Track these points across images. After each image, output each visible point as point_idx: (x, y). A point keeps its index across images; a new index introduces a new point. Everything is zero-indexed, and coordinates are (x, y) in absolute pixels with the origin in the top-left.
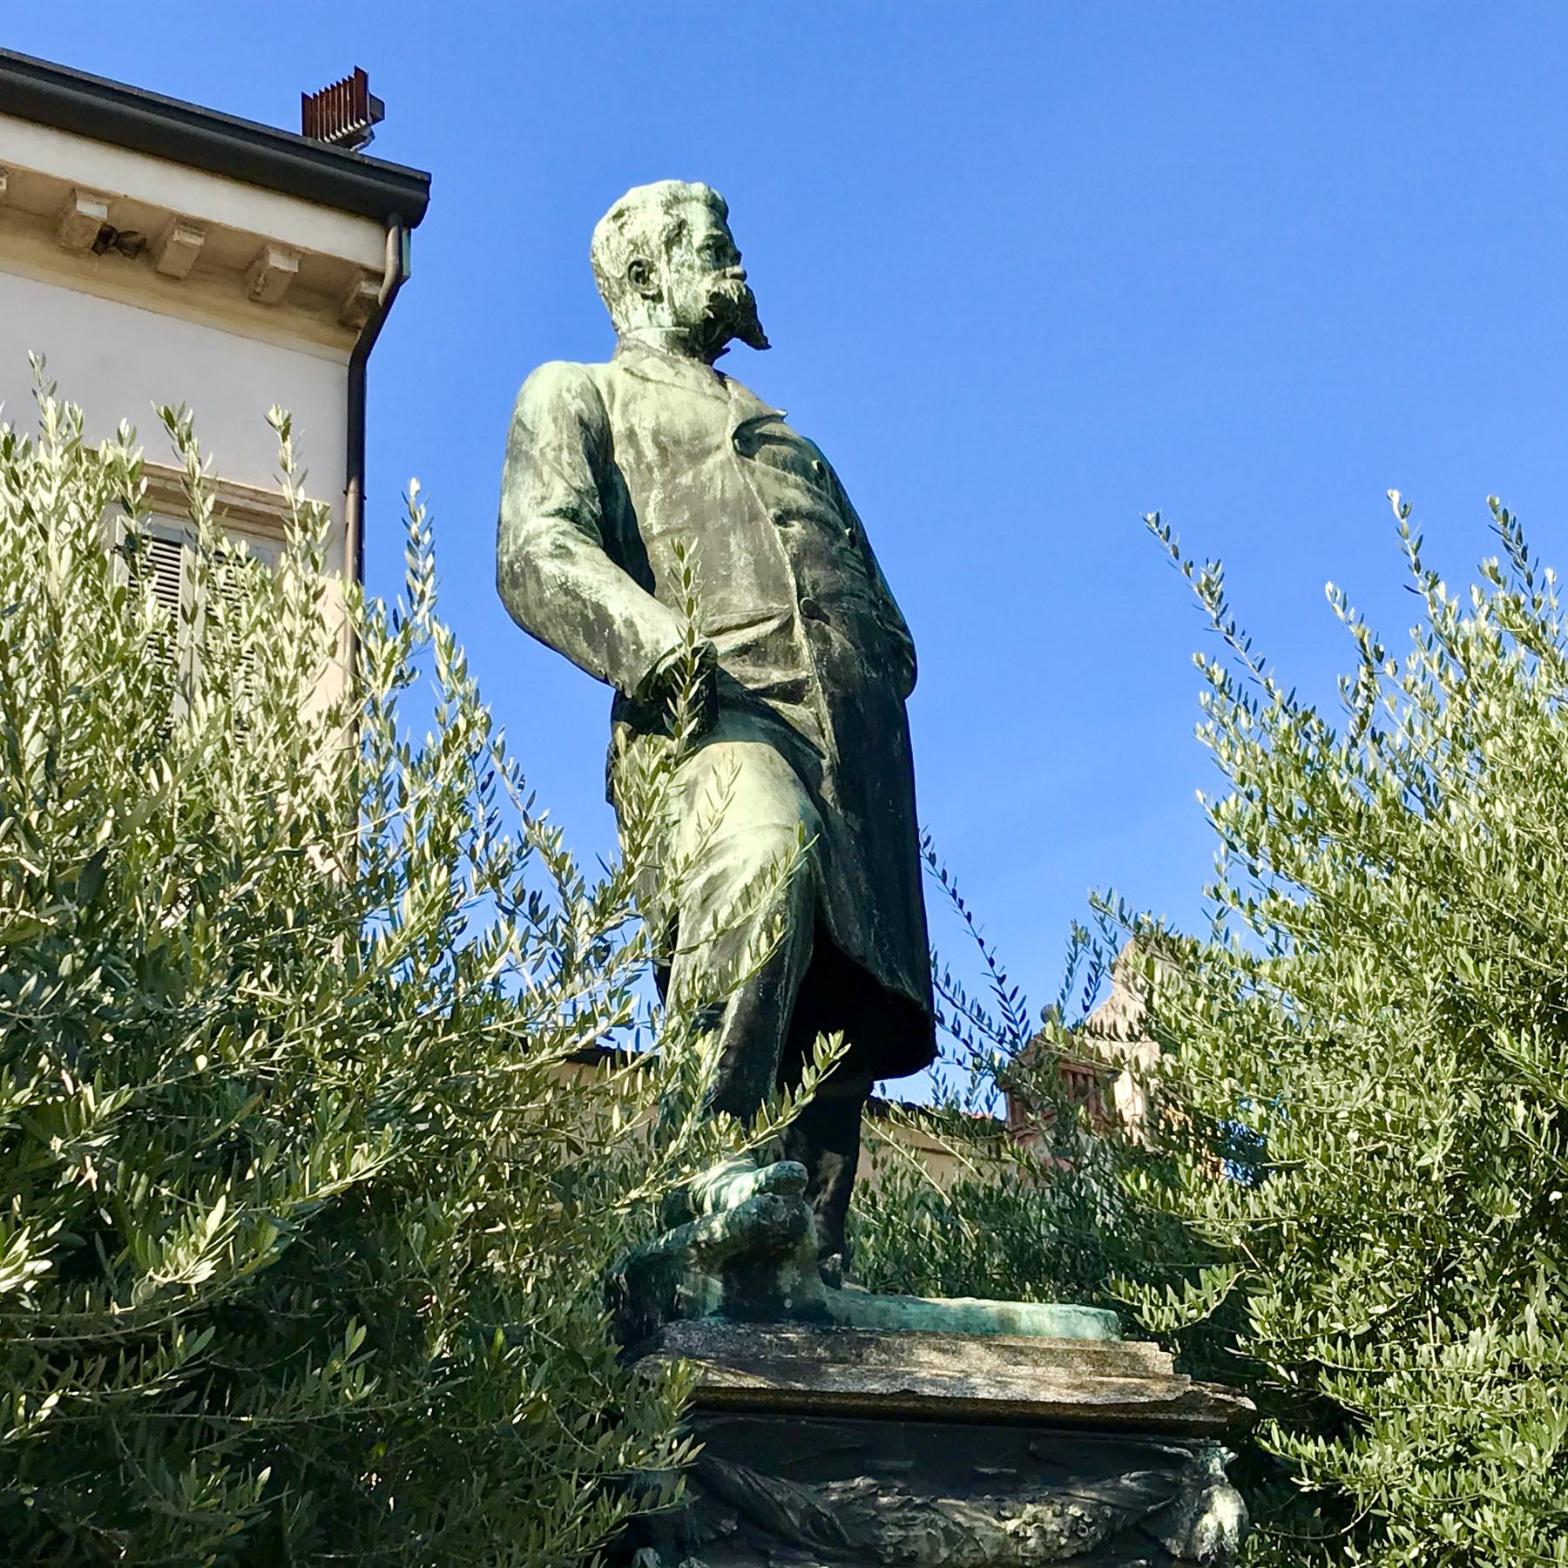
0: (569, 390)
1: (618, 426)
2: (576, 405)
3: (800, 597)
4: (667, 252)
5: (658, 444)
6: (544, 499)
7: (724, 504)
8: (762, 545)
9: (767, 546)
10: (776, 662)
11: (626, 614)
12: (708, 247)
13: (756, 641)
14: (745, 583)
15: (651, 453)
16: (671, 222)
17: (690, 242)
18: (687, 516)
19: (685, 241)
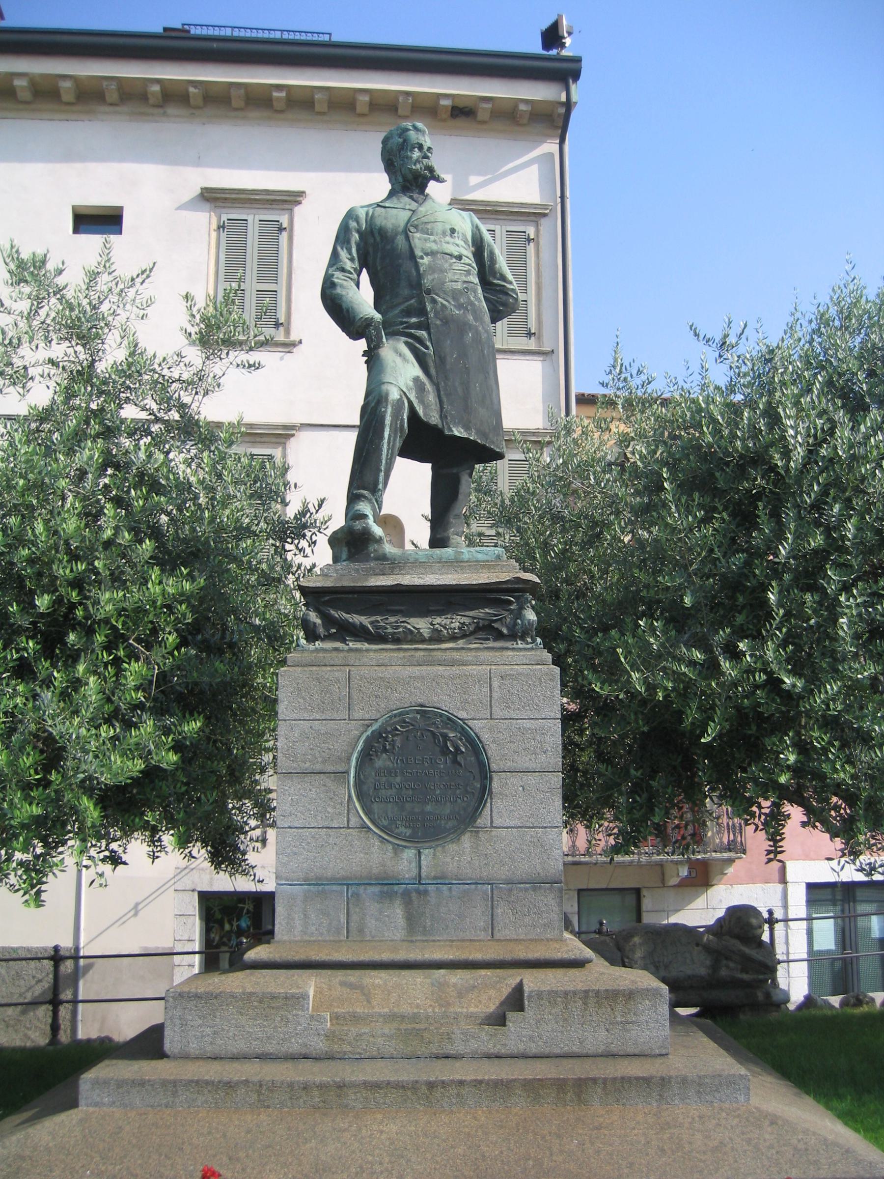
15: (378, 239)
16: (401, 140)
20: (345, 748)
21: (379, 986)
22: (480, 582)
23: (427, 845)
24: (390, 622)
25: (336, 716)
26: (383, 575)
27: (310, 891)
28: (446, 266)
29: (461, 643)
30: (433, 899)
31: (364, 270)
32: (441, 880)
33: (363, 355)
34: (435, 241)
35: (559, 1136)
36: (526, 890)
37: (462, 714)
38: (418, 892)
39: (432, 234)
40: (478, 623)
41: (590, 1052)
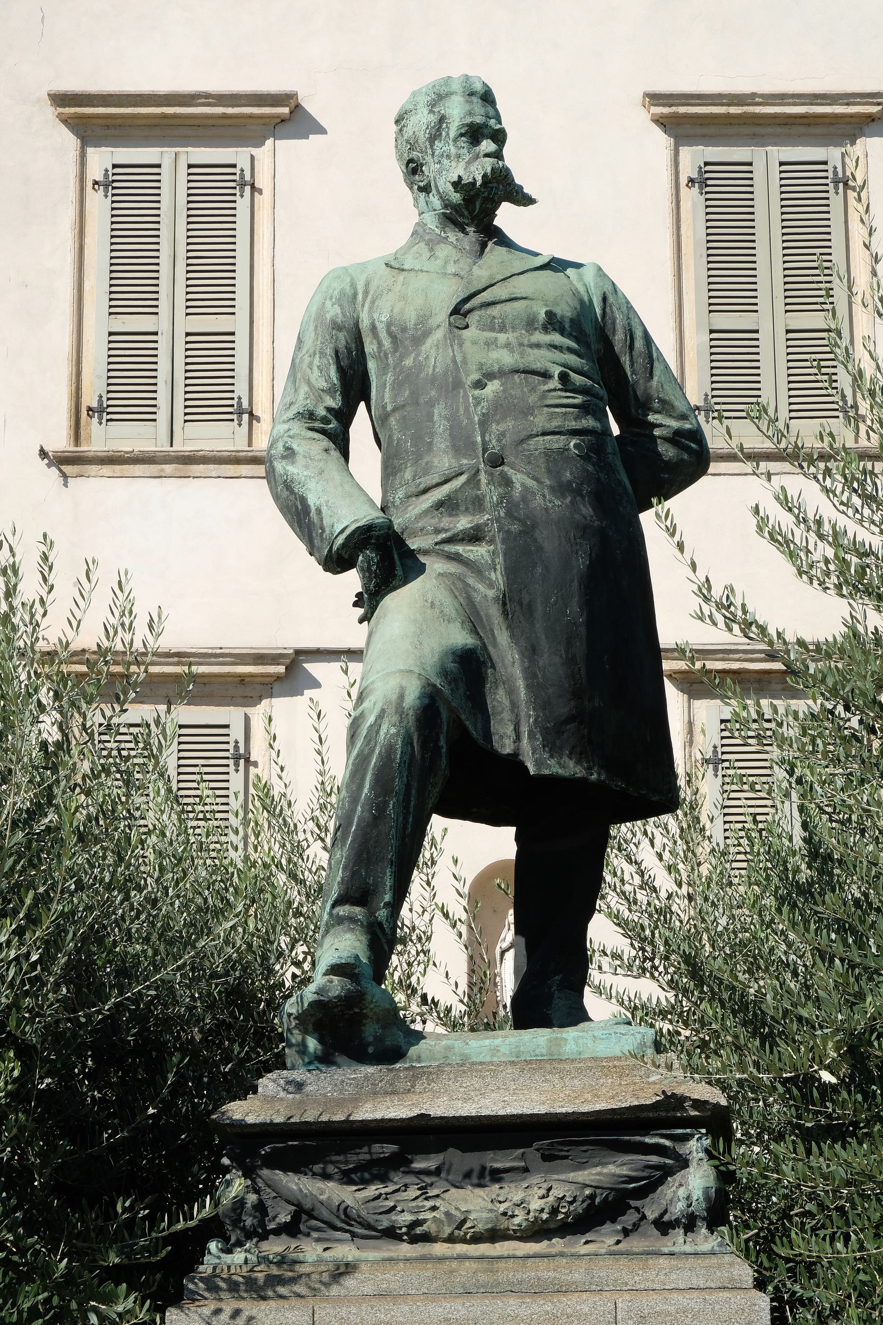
0: (331, 298)
1: (365, 324)
2: (333, 312)
3: (485, 450)
4: (432, 147)
5: (390, 334)
6: (291, 404)
7: (433, 379)
8: (458, 410)
9: (462, 411)
10: (467, 509)
11: (318, 503)
12: (462, 135)
13: (449, 496)
14: (443, 446)
15: (387, 343)
16: (433, 118)
17: (448, 134)
18: (407, 393)
19: (444, 133)
22: (598, 1107)
26: (394, 1093)
28: (532, 399)
29: (558, 1245)
31: (362, 405)
33: (356, 604)
34: (508, 345)
39: (502, 329)
40: (592, 1197)
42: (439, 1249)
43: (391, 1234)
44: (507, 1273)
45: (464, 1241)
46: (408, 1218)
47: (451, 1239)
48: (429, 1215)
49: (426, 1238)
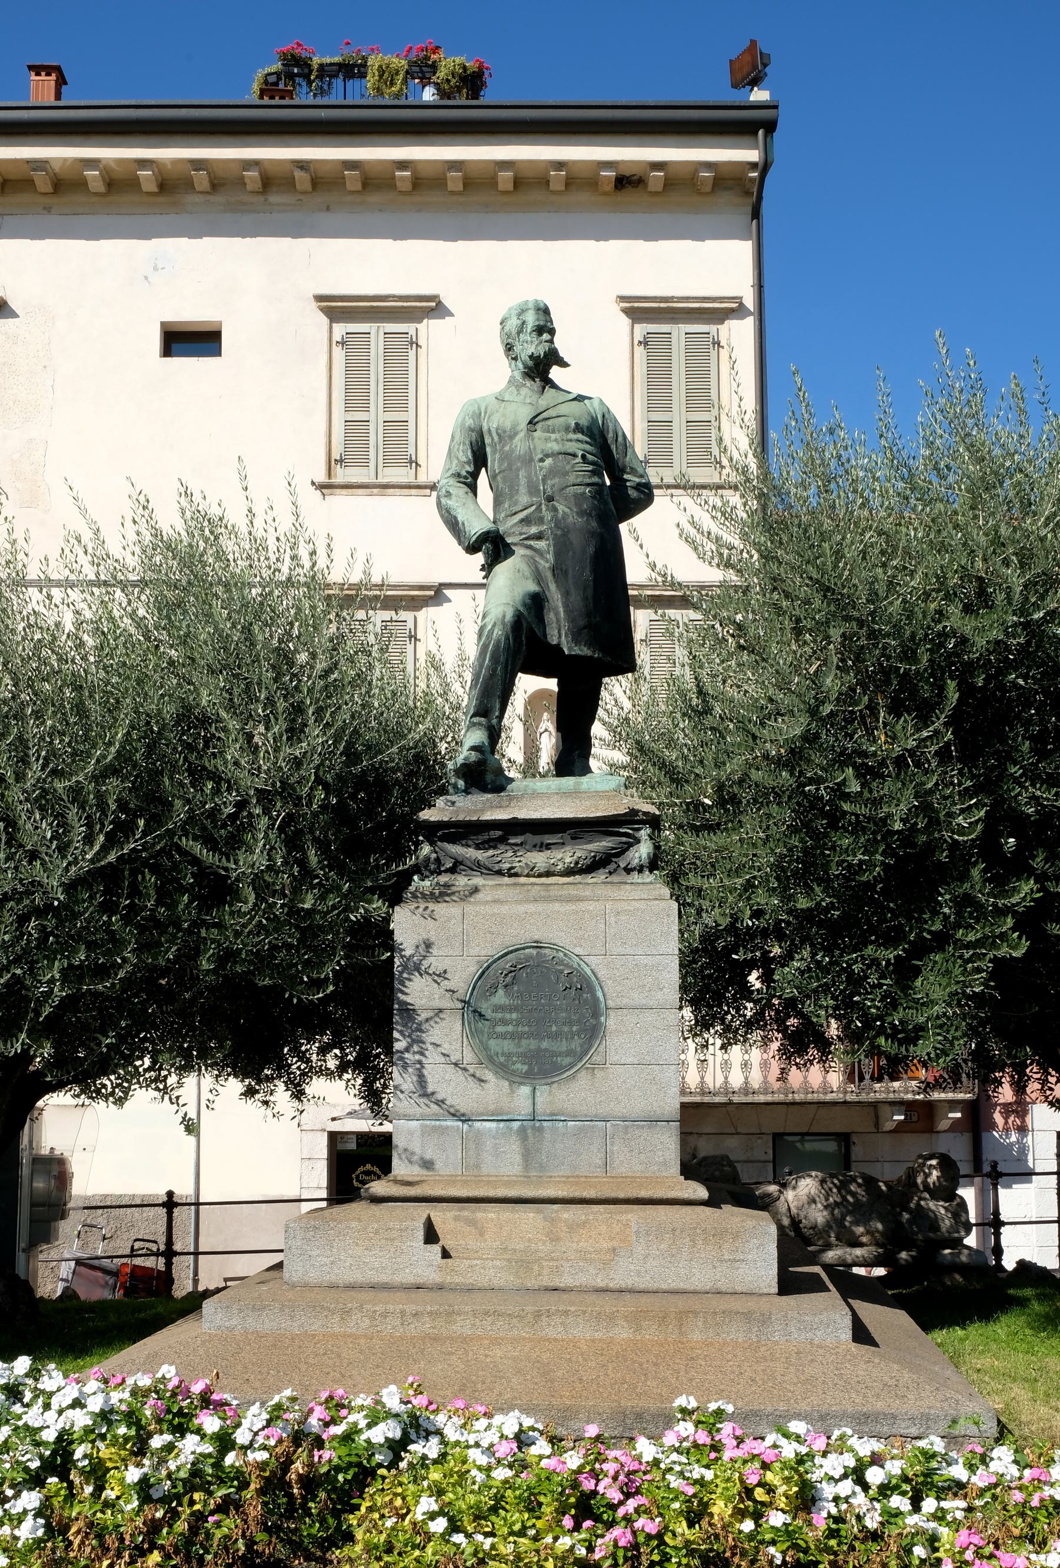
20: (462, 985)
21: (492, 1220)
23: (543, 1081)
24: (506, 857)
25: (451, 953)
27: (427, 1126)
30: (547, 1135)
32: (553, 1118)
35: (655, 1364)
36: (643, 1127)
37: (578, 951)
38: (533, 1128)
40: (595, 857)
41: (698, 1288)
42: (522, 880)
43: (500, 873)
44: (555, 892)
45: (534, 876)
46: (508, 865)
47: (528, 876)
48: (517, 865)
49: (516, 875)
